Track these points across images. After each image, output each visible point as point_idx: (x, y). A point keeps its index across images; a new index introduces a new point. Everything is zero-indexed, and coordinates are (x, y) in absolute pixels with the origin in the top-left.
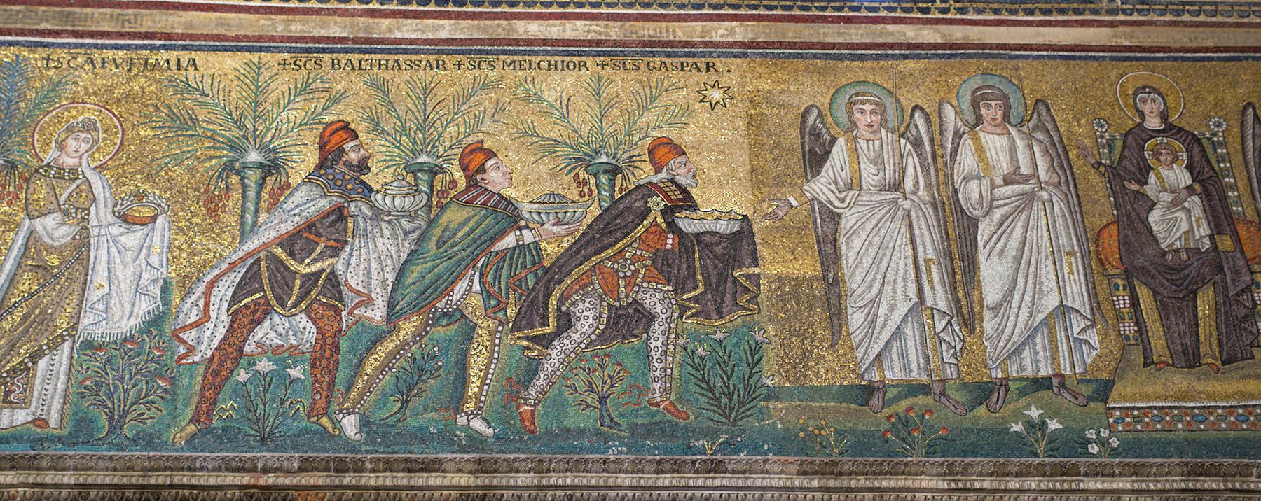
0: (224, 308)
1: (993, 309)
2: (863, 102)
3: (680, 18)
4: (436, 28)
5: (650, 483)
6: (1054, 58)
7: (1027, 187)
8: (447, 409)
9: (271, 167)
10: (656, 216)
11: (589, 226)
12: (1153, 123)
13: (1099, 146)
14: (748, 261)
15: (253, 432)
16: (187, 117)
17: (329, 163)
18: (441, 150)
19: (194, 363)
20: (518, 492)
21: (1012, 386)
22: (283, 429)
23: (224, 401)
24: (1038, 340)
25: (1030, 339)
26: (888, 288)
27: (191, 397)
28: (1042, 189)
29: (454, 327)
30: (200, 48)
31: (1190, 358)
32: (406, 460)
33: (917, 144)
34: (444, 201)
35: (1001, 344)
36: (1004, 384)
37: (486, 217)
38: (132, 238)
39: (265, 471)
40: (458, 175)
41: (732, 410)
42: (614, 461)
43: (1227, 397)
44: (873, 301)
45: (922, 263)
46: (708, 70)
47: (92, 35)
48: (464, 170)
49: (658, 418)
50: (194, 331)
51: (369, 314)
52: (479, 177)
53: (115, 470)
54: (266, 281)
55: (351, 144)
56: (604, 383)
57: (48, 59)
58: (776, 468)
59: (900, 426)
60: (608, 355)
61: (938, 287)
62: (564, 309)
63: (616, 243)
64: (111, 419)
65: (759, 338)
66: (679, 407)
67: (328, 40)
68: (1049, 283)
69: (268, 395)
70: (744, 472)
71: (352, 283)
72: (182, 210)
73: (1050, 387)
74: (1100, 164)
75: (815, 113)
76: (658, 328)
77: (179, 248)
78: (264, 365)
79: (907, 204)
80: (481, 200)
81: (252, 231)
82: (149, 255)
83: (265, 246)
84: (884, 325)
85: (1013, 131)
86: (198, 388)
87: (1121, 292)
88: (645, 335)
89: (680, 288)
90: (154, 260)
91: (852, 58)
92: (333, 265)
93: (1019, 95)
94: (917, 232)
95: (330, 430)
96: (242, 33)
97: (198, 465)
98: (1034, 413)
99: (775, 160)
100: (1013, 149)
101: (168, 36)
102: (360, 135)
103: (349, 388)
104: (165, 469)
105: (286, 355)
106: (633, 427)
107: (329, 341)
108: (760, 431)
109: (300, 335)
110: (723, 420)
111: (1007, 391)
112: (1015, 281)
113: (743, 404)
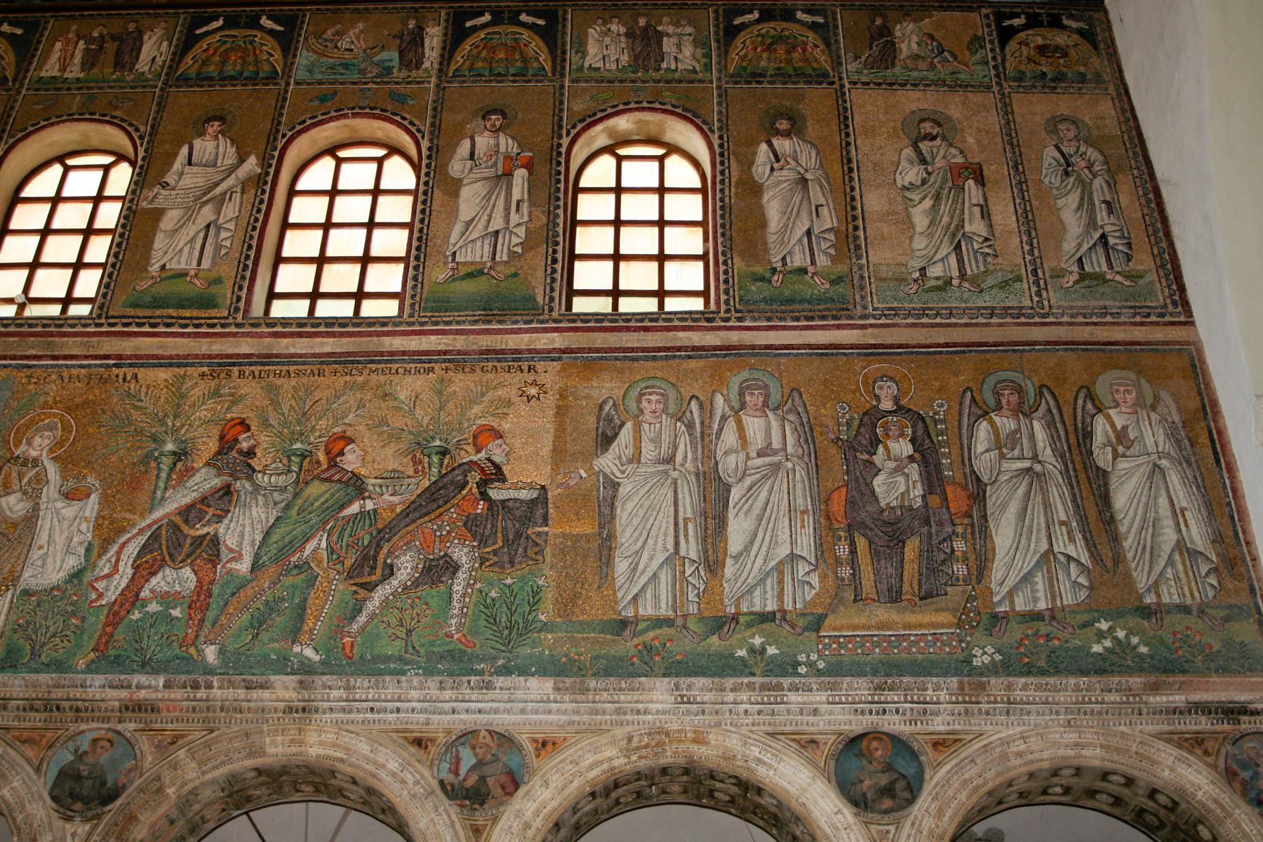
1: (734, 557)
2: (650, 394)
3: (512, 332)
4: (323, 344)
6: (811, 355)
7: (776, 459)
10: (472, 485)
11: (419, 496)
12: (887, 405)
13: (839, 425)
14: (540, 521)
21: (742, 619)
24: (769, 581)
25: (762, 581)
26: (650, 541)
28: (787, 460)
29: (303, 576)
30: (142, 366)
31: (894, 596)
33: (690, 426)
35: (738, 585)
36: (735, 618)
38: (70, 511)
39: (139, 687)
40: (322, 456)
43: (921, 626)
44: (637, 552)
45: (681, 521)
47: (65, 357)
51: (238, 566)
54: (164, 542)
56: (412, 619)
57: (30, 377)
59: (645, 653)
61: (692, 540)
64: (33, 648)
65: (541, 583)
67: (238, 356)
68: (784, 535)
71: (229, 543)
73: (773, 620)
74: (838, 439)
75: (611, 402)
76: (461, 575)
77: (103, 518)
78: (154, 607)
79: (675, 474)
80: (337, 477)
82: (80, 524)
83: (166, 515)
84: (643, 572)
85: (770, 414)
86: (100, 627)
87: (843, 542)
89: (483, 542)
90: (84, 527)
91: (646, 359)
92: (217, 530)
93: (778, 385)
94: (680, 496)
96: (174, 352)
98: (757, 641)
100: (768, 430)
101: (119, 357)
106: (430, 655)
107: (205, 588)
111: (737, 623)
112: (755, 535)
113: (521, 635)
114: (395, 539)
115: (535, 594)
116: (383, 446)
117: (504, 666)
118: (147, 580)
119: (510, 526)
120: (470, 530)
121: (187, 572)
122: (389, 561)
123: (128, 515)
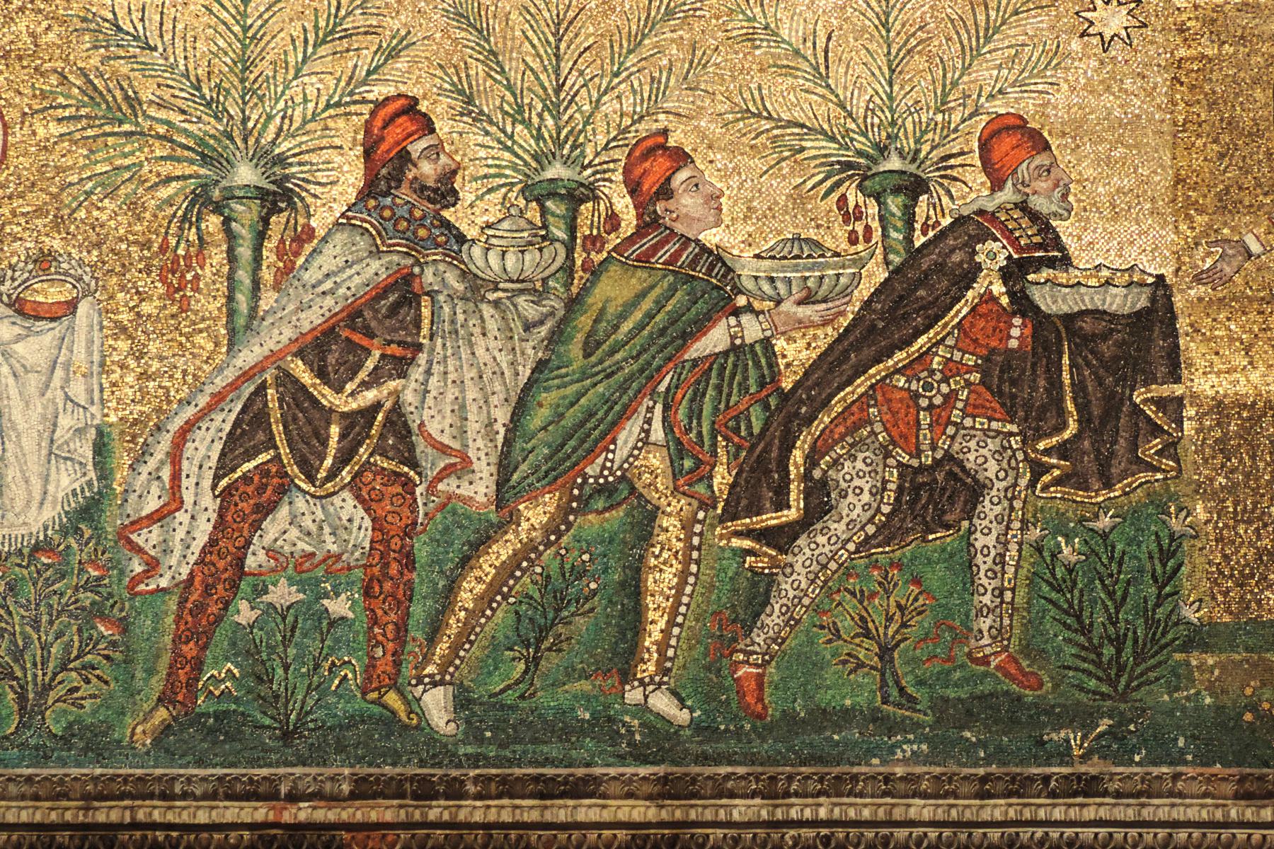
0: (207, 483)
5: (968, 816)
8: (607, 673)
9: (277, 197)
11: (867, 304)
15: (267, 721)
16: (118, 94)
18: (589, 151)
19: (159, 590)
20: (732, 832)
22: (319, 714)
23: (216, 663)
27: (158, 657)
29: (620, 513)
32: (536, 779)
34: (597, 258)
37: (673, 290)
39: (293, 798)
40: (624, 205)
41: (1121, 669)
42: (901, 778)
48: (632, 193)
49: (986, 687)
50: (156, 528)
51: (466, 490)
53: (36, 798)
54: (277, 429)
55: (423, 144)
56: (890, 619)
58: (1195, 788)
60: (899, 565)
62: (817, 474)
63: (918, 334)
64: (22, 698)
66: (1025, 663)
69: (292, 651)
70: (1138, 795)
71: (433, 428)
72: (123, 288)
76: (990, 508)
78: (283, 593)
81: (248, 327)
82: (67, 380)
83: (274, 357)
86: (168, 639)
88: (965, 524)
90: (78, 389)
92: (396, 394)
95: (403, 716)
97: (178, 789)
99: (1222, 156)
103: (432, 639)
104: (122, 797)
105: (320, 573)
106: (941, 706)
107: (396, 543)
108: (1171, 713)
109: (341, 532)
110: (1104, 689)
115: (1166, 555)
117: (1110, 732)
118: (256, 526)
122: (817, 474)
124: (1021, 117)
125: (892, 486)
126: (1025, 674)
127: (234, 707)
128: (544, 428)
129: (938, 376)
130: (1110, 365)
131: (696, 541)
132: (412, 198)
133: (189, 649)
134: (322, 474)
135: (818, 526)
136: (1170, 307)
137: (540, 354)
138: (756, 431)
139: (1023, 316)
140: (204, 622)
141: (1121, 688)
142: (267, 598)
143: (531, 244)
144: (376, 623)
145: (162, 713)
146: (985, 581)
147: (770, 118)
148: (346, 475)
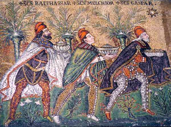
0: (14, 83)
9: (21, 38)
11: (120, 55)
17: (39, 36)
29: (83, 88)
34: (75, 48)
41: (166, 111)
46: (150, 5)
48: (80, 38)
49: (146, 115)
51: (57, 84)
52: (85, 40)
54: (25, 74)
60: (129, 95)
63: (128, 60)
69: (31, 110)
71: (51, 74)
76: (143, 87)
78: (28, 101)
80: (86, 47)
83: (23, 63)
86: (9, 109)
88: (139, 89)
92: (45, 69)
102: (47, 26)
106: (139, 118)
107: (47, 93)
110: (164, 115)
114: (115, 72)
116: (101, 35)
118: (23, 90)
119: (156, 67)
120: (142, 69)
121: (37, 86)
123: (7, 63)
124: (140, 27)
125: (127, 83)
126: (152, 113)
127: (21, 119)
128: (69, 74)
129: (132, 66)
130: (159, 64)
131: (96, 92)
132: (44, 38)
133: (13, 110)
134: (33, 82)
135: (116, 89)
136: (167, 56)
137: (68, 63)
138: (104, 75)
139: (144, 57)
140: (15, 106)
141: (167, 114)
142: (25, 102)
143: (64, 45)
144: (44, 105)
145: (9, 121)
146: (143, 98)
147: (101, 26)
148: (37, 82)
